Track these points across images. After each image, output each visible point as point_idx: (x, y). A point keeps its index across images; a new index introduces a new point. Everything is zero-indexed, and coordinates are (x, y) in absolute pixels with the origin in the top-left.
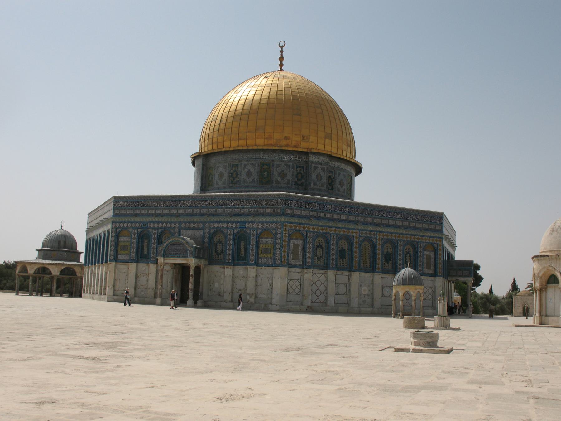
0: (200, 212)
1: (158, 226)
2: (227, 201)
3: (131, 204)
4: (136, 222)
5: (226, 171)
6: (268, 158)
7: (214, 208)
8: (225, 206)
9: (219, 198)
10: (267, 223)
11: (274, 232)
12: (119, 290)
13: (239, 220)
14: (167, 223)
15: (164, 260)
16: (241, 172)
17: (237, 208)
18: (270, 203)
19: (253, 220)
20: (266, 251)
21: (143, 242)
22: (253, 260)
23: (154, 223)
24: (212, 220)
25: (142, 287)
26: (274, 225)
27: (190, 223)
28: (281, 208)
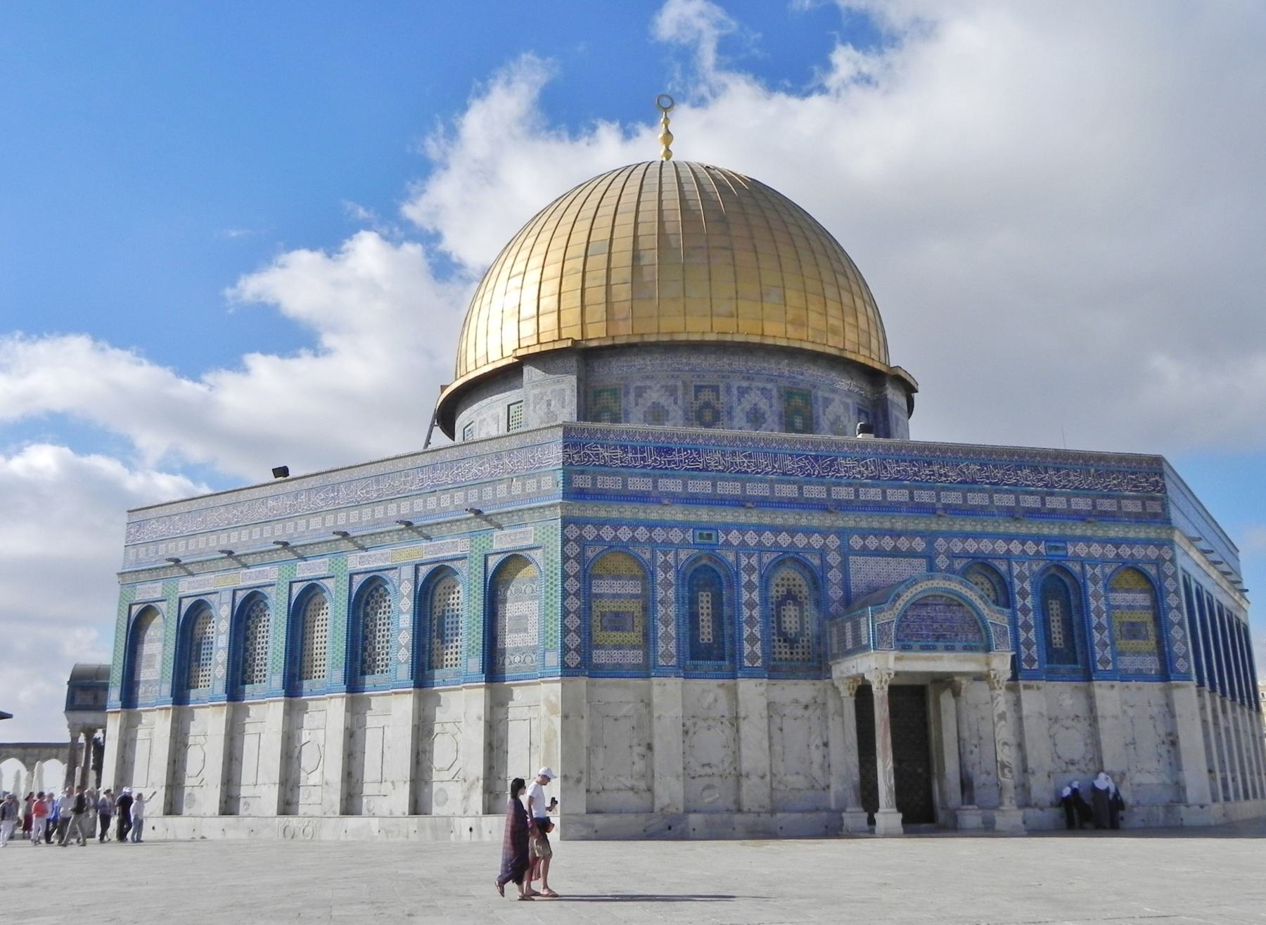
0: (912, 498)
1: (760, 543)
2: (995, 467)
3: (643, 459)
4: (667, 526)
5: (676, 403)
6: (801, 377)
7: (954, 490)
8: (991, 483)
9: (967, 459)
10: (1132, 543)
11: (1152, 571)
12: (603, 789)
13: (1046, 531)
14: (792, 531)
15: (897, 659)
16: (731, 408)
17: (1032, 493)
18: (1128, 482)
19: (1089, 533)
20: (1133, 631)
21: (693, 601)
22: (1107, 662)
23: (742, 529)
24: (957, 528)
25: (708, 770)
26: (1152, 552)
27: (879, 533)
28: (1162, 499)
